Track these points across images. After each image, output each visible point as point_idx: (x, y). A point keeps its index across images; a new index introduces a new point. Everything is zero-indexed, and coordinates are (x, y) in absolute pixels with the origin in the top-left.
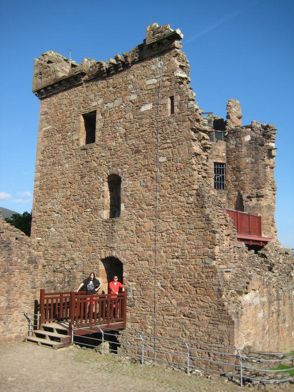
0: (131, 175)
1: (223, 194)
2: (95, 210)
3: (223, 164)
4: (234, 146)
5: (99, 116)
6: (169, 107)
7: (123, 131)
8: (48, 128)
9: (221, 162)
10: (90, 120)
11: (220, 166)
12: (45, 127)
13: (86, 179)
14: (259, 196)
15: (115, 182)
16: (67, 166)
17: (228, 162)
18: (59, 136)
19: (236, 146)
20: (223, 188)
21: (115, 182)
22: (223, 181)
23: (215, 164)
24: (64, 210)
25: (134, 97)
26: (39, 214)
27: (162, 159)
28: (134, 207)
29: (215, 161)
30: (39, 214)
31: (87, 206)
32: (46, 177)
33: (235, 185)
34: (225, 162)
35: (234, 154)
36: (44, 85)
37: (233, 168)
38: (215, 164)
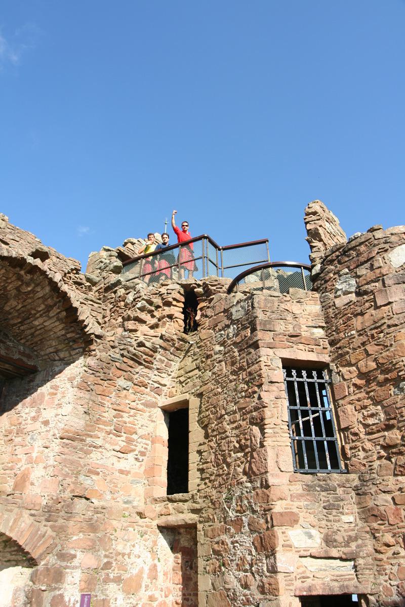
1: (340, 491)
3: (320, 367)
4: (353, 297)
9: (312, 357)
11: (310, 376)
17: (341, 358)
19: (358, 294)
20: (335, 465)
22: (330, 433)
23: (289, 365)
29: (287, 354)
33: (386, 447)
34: (326, 358)
35: (357, 322)
37: (365, 376)
38: (289, 365)
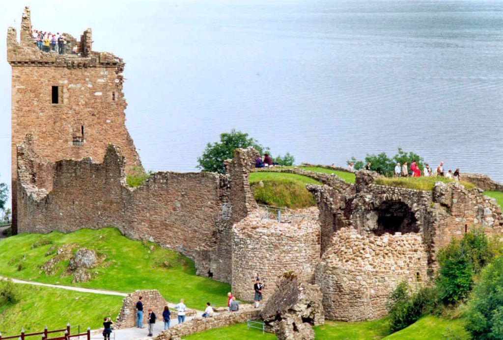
0: (90, 126)
2: (67, 141)
5: (65, 90)
6: (112, 96)
7: (84, 103)
8: (22, 87)
12: (18, 86)
13: (58, 124)
16: (41, 114)
18: (32, 95)
24: (41, 139)
25: (90, 86)
26: (19, 140)
27: (108, 121)
28: (92, 142)
30: (19, 140)
31: (59, 138)
32: (23, 118)
36: (19, 60)
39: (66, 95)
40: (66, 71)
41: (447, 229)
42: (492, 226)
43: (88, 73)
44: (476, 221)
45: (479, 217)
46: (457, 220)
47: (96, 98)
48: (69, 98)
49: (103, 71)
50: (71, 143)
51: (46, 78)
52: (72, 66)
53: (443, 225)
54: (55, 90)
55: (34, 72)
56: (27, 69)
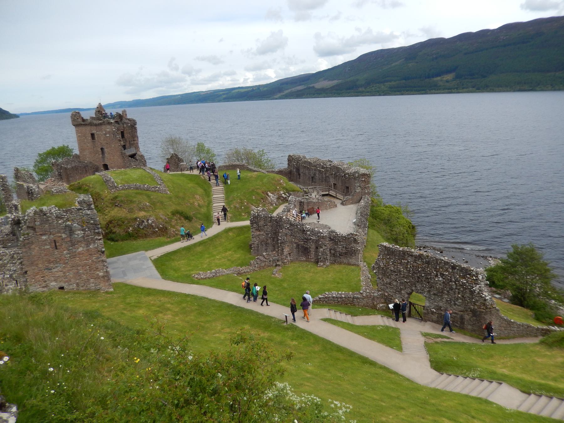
10: (93, 135)
14: (134, 140)
15: (102, 149)
21: (102, 149)
39: (96, 137)
40: (95, 127)
41: (33, 246)
42: (83, 237)
43: (103, 127)
44: (64, 236)
45: (68, 232)
46: (44, 237)
47: (107, 137)
48: (97, 138)
49: (108, 127)
50: (101, 156)
51: (88, 130)
52: (96, 125)
53: (28, 243)
54: (93, 135)
55: (83, 129)
56: (81, 128)
